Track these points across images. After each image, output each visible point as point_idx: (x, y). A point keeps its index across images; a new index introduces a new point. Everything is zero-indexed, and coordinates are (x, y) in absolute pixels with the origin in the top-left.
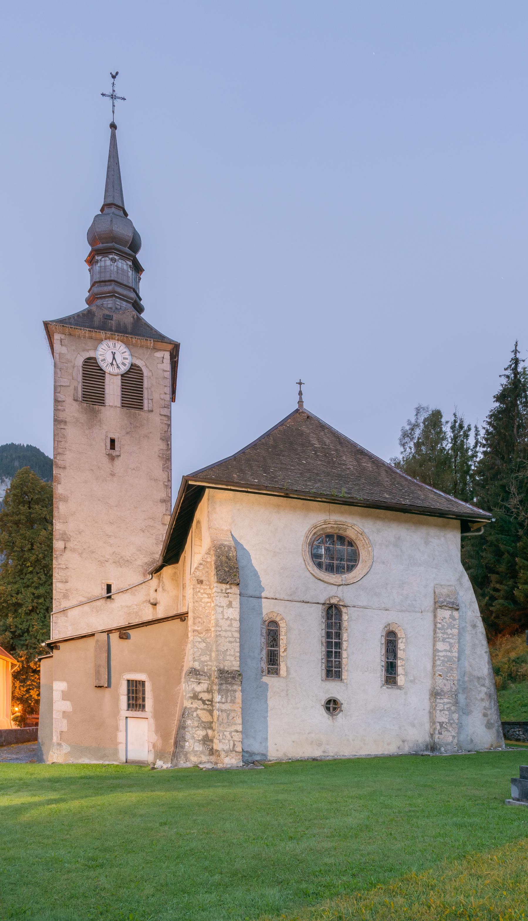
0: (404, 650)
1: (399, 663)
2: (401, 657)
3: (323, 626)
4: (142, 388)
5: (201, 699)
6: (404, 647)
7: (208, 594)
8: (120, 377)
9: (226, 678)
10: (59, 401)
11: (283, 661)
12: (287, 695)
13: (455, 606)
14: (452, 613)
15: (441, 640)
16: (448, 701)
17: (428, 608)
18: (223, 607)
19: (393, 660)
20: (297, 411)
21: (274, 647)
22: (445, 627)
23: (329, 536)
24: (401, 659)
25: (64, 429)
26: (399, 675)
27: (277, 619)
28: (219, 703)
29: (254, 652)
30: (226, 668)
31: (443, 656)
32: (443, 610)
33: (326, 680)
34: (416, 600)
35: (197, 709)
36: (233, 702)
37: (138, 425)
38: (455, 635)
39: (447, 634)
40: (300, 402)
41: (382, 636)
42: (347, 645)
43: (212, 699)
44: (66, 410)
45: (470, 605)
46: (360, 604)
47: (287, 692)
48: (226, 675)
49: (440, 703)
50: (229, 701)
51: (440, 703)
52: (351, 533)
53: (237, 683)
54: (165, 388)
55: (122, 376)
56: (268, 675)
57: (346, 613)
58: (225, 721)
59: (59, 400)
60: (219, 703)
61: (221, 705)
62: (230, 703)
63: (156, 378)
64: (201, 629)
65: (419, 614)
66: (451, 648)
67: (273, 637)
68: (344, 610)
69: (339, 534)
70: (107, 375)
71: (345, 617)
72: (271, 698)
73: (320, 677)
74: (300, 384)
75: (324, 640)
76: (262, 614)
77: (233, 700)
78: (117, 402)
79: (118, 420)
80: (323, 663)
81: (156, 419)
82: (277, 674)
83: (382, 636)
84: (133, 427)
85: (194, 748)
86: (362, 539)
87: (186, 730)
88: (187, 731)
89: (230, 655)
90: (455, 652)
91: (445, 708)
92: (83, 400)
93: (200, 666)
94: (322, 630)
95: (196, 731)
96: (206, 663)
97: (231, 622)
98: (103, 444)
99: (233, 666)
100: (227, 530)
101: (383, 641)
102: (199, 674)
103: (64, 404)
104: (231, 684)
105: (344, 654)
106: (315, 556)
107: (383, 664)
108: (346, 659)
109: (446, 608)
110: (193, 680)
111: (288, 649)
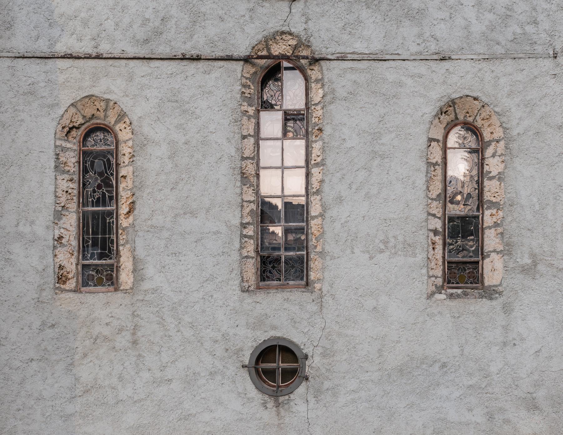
0: (500, 177)
2: (494, 200)
26: (488, 256)
27: (111, 120)
34: (535, 23)
41: (431, 140)
42: (320, 177)
46: (360, 47)
65: (548, 64)
67: (101, 174)
80: (250, 237)
83: (431, 140)
94: (244, 137)
107: (438, 224)
111: (137, 206)
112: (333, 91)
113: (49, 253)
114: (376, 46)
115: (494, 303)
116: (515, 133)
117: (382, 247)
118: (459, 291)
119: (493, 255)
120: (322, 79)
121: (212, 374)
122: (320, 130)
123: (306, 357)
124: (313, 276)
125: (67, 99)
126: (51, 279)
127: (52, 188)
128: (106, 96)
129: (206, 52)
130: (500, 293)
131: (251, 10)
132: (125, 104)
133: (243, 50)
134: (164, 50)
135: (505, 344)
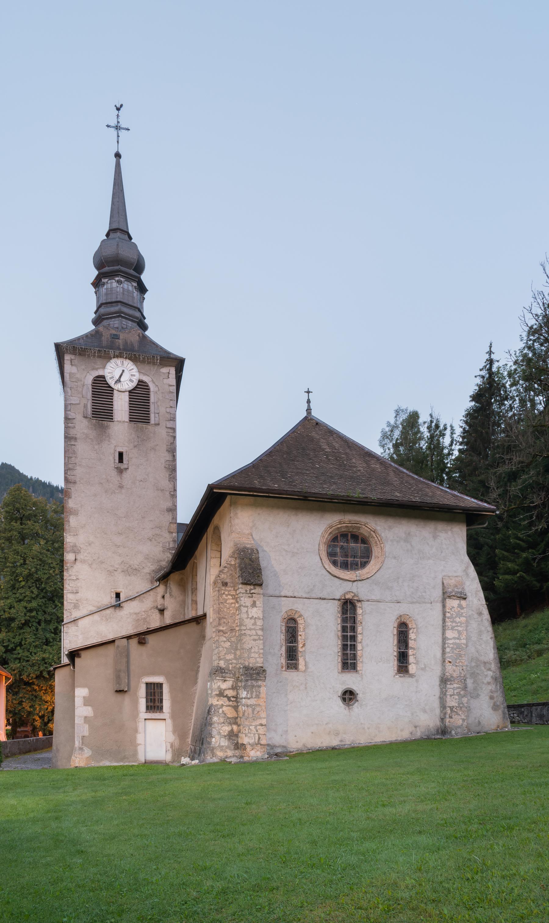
0: (415, 640)
1: (410, 652)
3: (339, 621)
4: (149, 403)
5: (226, 696)
6: (415, 637)
7: (232, 595)
8: (127, 393)
9: (251, 675)
10: (69, 419)
11: (302, 656)
12: (306, 688)
13: (463, 595)
14: (460, 602)
15: (450, 628)
16: (458, 686)
17: (437, 599)
18: (247, 607)
19: (405, 650)
20: (306, 418)
21: (292, 643)
22: (454, 616)
23: (344, 536)
24: (412, 648)
25: (74, 445)
27: (296, 617)
28: (244, 698)
29: (274, 649)
30: (251, 665)
31: (452, 644)
32: (451, 600)
33: (342, 672)
34: (425, 592)
35: (222, 706)
36: (258, 697)
37: (145, 438)
38: (463, 623)
39: (455, 622)
40: (309, 410)
41: (394, 627)
42: (361, 638)
43: (237, 695)
44: (76, 426)
45: (476, 594)
46: (373, 597)
47: (306, 685)
48: (251, 672)
49: (450, 688)
50: (254, 697)
51: (450, 688)
52: (364, 531)
53: (261, 679)
54: (171, 402)
55: (130, 392)
56: (287, 670)
57: (360, 607)
58: (251, 716)
59: (70, 417)
60: (244, 698)
61: (247, 700)
62: (255, 698)
63: (162, 393)
64: (226, 629)
65: (429, 605)
66: (459, 636)
67: (291, 633)
68: (358, 605)
69: (353, 532)
70: (115, 392)
71: (359, 611)
72: (291, 692)
73: (337, 670)
74: (308, 392)
75: (340, 634)
76: (281, 612)
77: (258, 696)
78: (126, 418)
79: (126, 435)
81: (162, 432)
82: (296, 669)
84: (141, 441)
85: (220, 743)
86: (375, 536)
87: (213, 726)
88: (213, 728)
89: (254, 652)
90: (464, 639)
91: (455, 693)
92: (93, 417)
93: (225, 664)
94: (338, 624)
95: (222, 727)
96: (230, 662)
97: (255, 620)
98: (111, 458)
99: (258, 663)
100: (248, 534)
101: (395, 632)
102: (224, 672)
103: (74, 421)
104: (257, 680)
105: (359, 647)
106: (331, 555)
107: (395, 654)
108: (361, 652)
109: (455, 598)
110: (219, 678)
111: (306, 644)
112: (365, 611)
113: (279, 659)
114: (378, 598)
115: (413, 679)
116: (420, 626)
117: (380, 660)
118: (402, 675)
119: (412, 664)
120: (362, 607)
121: (329, 699)
122: (361, 623)
123: (358, 694)
124: (358, 669)
125: (284, 610)
126: (280, 667)
127: (280, 638)
128: (296, 610)
129: (327, 597)
130: (415, 676)
131: (340, 584)
132: (302, 612)
133: (338, 597)
134: (314, 596)
135: (416, 692)
